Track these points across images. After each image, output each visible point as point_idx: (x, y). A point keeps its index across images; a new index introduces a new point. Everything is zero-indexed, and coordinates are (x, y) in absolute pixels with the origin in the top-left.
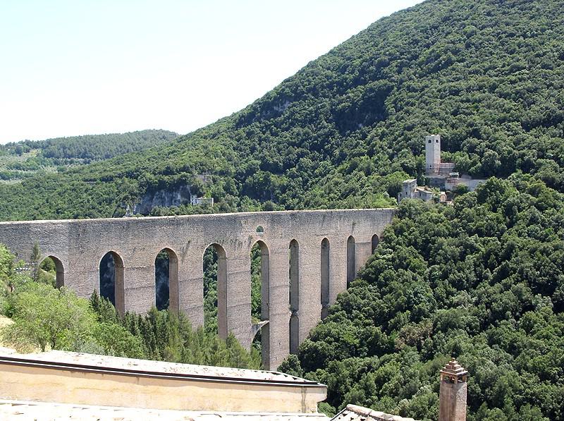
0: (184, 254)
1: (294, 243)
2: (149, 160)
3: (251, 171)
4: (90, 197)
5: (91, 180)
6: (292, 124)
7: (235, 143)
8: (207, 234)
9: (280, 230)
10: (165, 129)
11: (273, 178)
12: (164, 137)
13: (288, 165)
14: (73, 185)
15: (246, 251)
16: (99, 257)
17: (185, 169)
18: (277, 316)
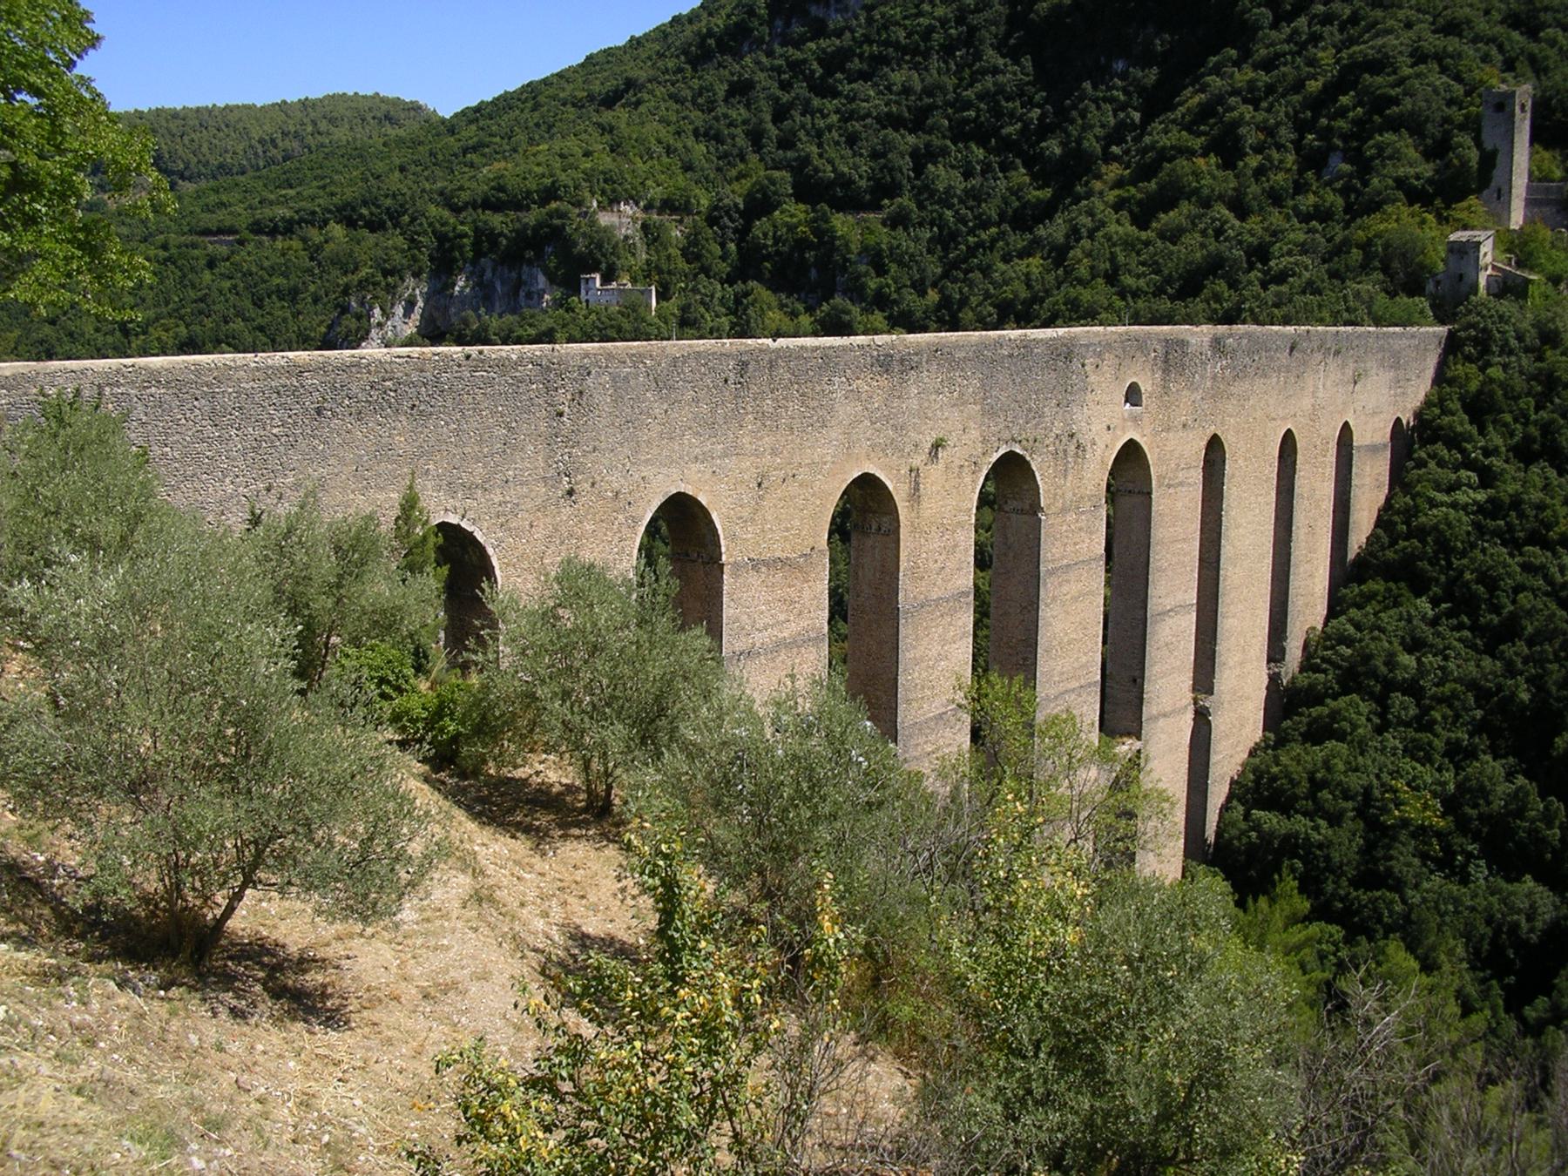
0: (915, 494)
1: (1215, 447)
2: (402, 169)
3: (760, 204)
4: (227, 284)
5: (220, 231)
6: (880, 60)
7: (698, 117)
8: (990, 412)
9: (1186, 400)
10: (389, 92)
11: (842, 223)
12: (388, 117)
13: (884, 189)
14: (165, 247)
15: (1095, 473)
16: (636, 520)
17: (550, 194)
18: (1162, 722)
